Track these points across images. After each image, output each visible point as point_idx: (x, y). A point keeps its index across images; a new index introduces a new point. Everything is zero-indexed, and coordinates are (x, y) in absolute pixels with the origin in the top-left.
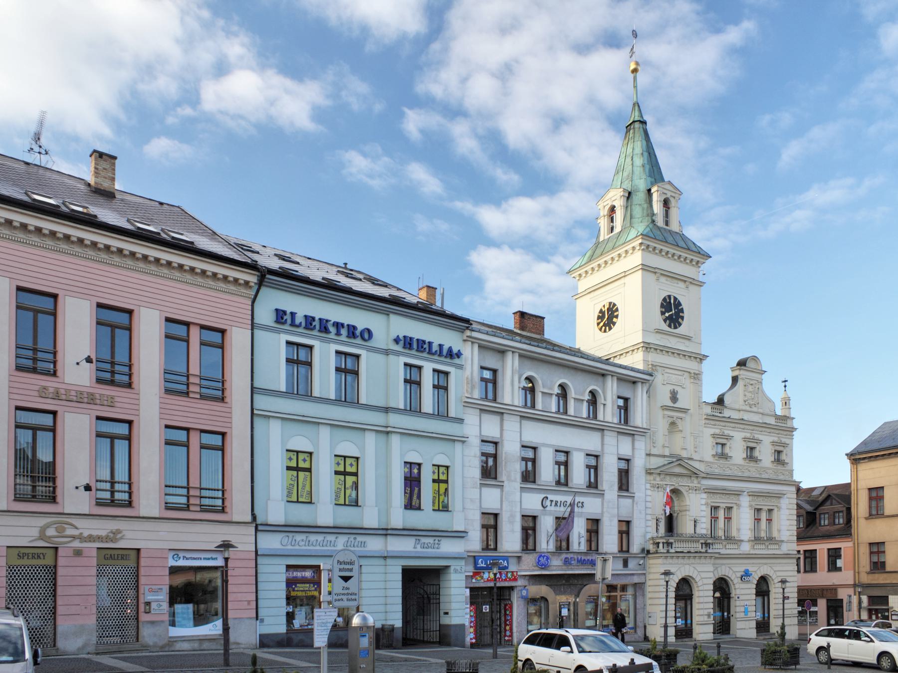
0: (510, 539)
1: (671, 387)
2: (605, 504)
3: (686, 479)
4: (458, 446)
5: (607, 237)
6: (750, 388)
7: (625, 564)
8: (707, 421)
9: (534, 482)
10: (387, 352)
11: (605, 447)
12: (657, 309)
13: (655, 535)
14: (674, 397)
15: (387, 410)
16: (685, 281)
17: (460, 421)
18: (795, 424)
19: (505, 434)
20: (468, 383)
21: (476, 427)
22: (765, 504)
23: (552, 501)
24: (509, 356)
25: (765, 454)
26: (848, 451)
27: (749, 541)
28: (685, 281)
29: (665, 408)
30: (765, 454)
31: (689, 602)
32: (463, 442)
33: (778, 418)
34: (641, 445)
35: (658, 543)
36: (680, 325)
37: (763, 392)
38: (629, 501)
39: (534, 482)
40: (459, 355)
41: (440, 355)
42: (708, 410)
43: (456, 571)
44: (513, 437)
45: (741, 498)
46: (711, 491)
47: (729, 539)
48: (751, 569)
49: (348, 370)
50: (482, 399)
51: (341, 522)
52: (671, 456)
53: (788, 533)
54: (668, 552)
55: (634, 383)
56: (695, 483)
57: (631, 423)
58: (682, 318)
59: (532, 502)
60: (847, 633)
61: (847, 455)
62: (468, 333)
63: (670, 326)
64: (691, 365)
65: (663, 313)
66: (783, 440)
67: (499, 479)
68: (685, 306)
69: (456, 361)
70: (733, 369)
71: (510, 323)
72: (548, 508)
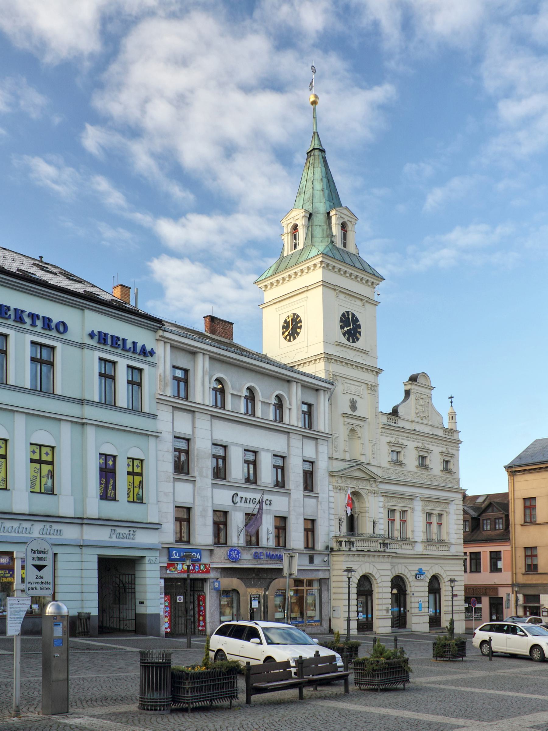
0: (203, 533)
1: (352, 397)
2: (292, 504)
4: (152, 440)
5: (290, 253)
6: (421, 402)
7: (311, 560)
8: (384, 430)
9: (225, 479)
10: (82, 346)
11: (291, 448)
12: (337, 324)
13: (338, 534)
14: (353, 406)
15: (82, 402)
16: (362, 300)
17: (154, 416)
18: (461, 437)
19: (197, 431)
20: (160, 381)
21: (170, 424)
22: (436, 509)
23: (241, 498)
24: (200, 357)
25: (435, 463)
26: (506, 464)
27: (422, 542)
28: (362, 300)
29: (345, 415)
30: (435, 463)
31: (369, 598)
32: (157, 437)
33: (445, 430)
34: (324, 448)
35: (341, 542)
36: (358, 339)
37: (432, 406)
38: (314, 501)
39: (225, 479)
40: (152, 353)
41: (134, 352)
42: (384, 419)
43: (151, 562)
44: (205, 435)
46: (388, 495)
47: (404, 540)
48: (424, 568)
49: (43, 360)
50: (174, 397)
51: (36, 510)
52: (351, 460)
53: (456, 536)
54: (350, 550)
55: (317, 390)
56: (373, 487)
57: (315, 427)
58: (360, 333)
59: (223, 498)
60: (505, 628)
61: (505, 467)
62: (160, 333)
64: (368, 377)
65: (342, 328)
66: (451, 451)
67: (191, 474)
68: (361, 322)
69: (149, 359)
70: (405, 384)
71: (201, 326)
72: (238, 505)
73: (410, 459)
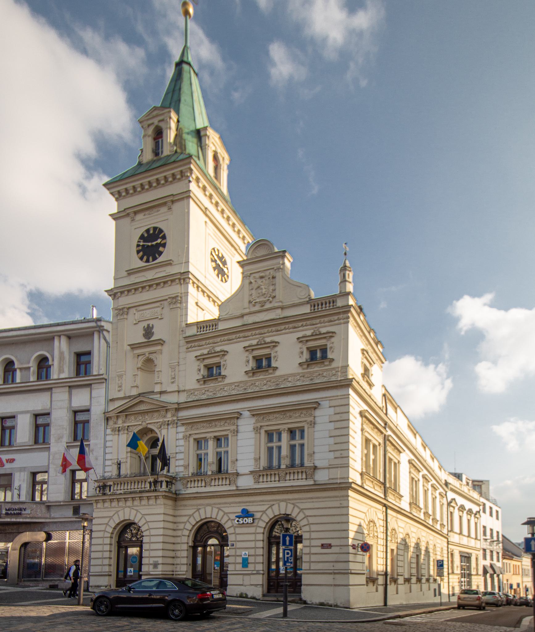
1: (145, 324)
3: (156, 414)
8: (189, 345)
14: (148, 332)
29: (133, 347)
34: (99, 392)
45: (241, 422)
56: (169, 417)
63: (147, 261)
73: (236, 365)
